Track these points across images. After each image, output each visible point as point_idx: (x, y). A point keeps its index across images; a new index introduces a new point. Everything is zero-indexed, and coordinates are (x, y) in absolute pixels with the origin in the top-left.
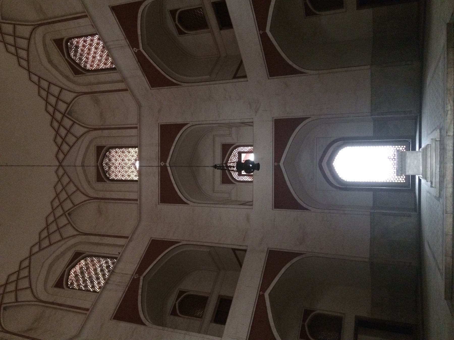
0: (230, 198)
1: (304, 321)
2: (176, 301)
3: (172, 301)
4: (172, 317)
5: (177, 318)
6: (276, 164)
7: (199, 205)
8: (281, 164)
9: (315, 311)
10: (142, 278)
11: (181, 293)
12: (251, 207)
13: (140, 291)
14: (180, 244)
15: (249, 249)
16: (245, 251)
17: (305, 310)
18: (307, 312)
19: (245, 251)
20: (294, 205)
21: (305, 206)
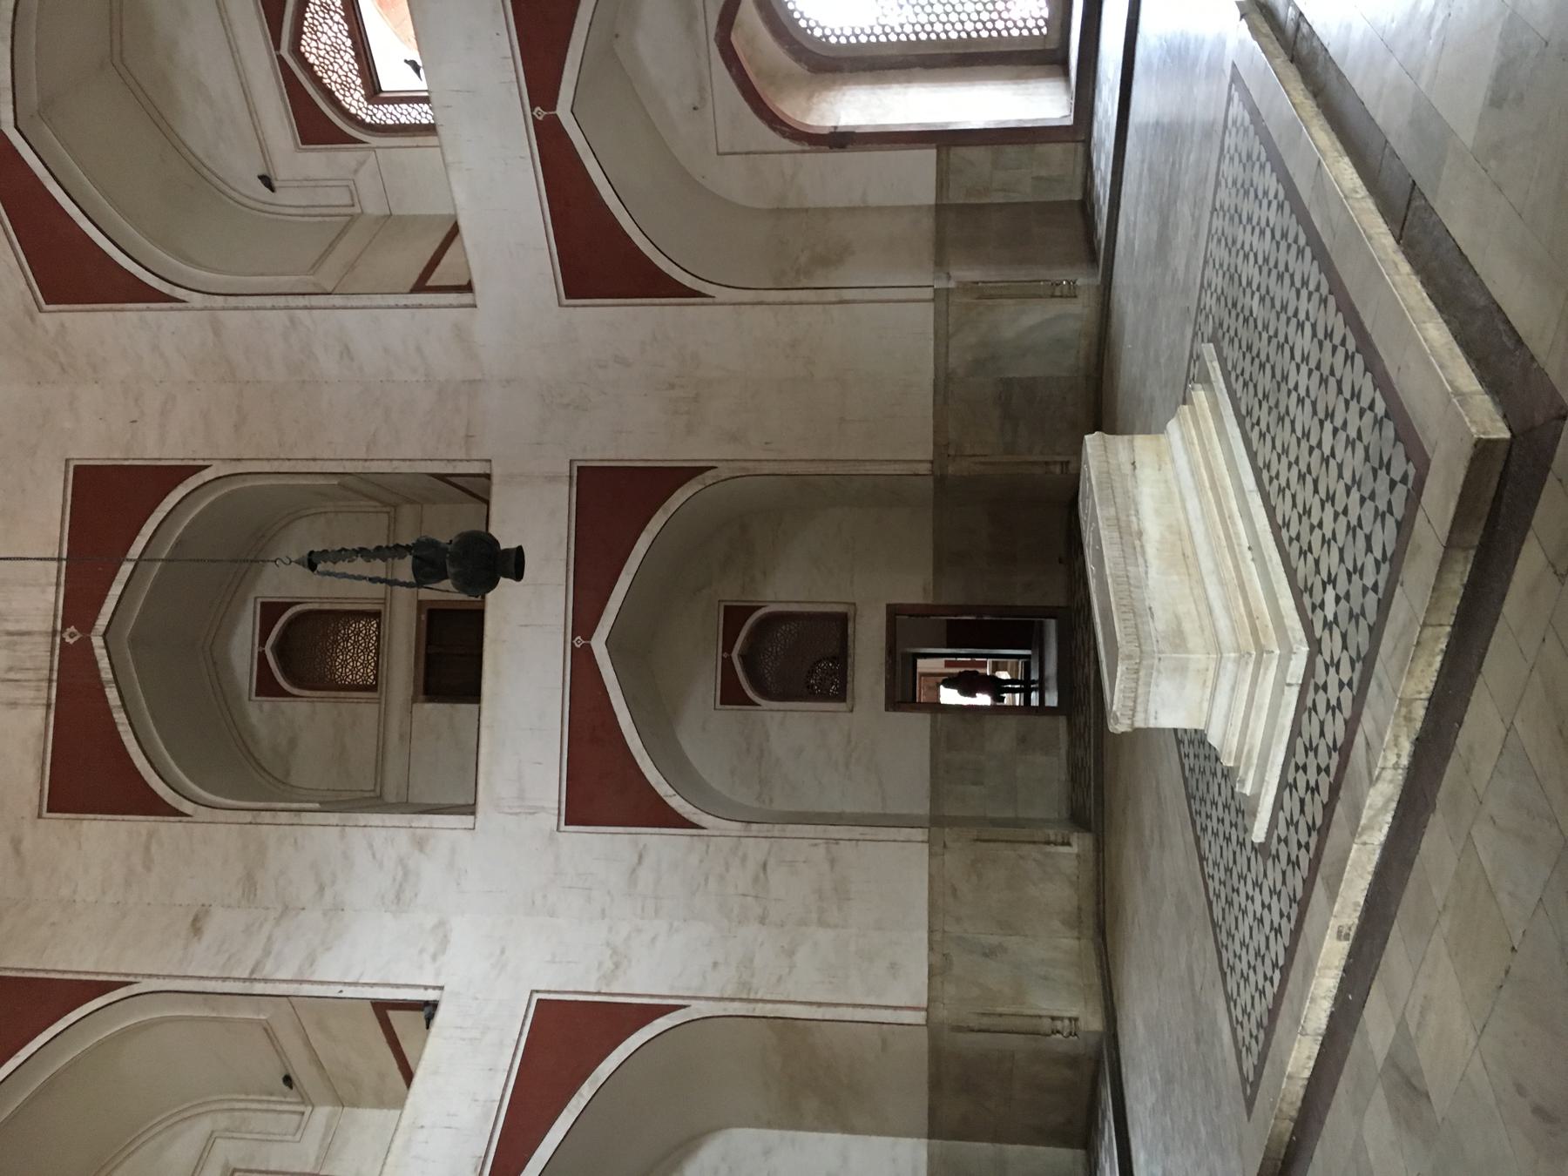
0: (357, 210)
1: (728, 648)
2: (263, 642)
3: (243, 647)
4: (268, 703)
5: (284, 704)
6: (541, 113)
7: (232, 301)
8: (563, 111)
9: (759, 608)
10: (97, 642)
11: (270, 612)
12: (465, 298)
13: (112, 694)
14: (207, 475)
15: (497, 473)
16: (488, 476)
17: (726, 608)
18: (734, 616)
19: (488, 476)
20: (649, 283)
21: (687, 280)
